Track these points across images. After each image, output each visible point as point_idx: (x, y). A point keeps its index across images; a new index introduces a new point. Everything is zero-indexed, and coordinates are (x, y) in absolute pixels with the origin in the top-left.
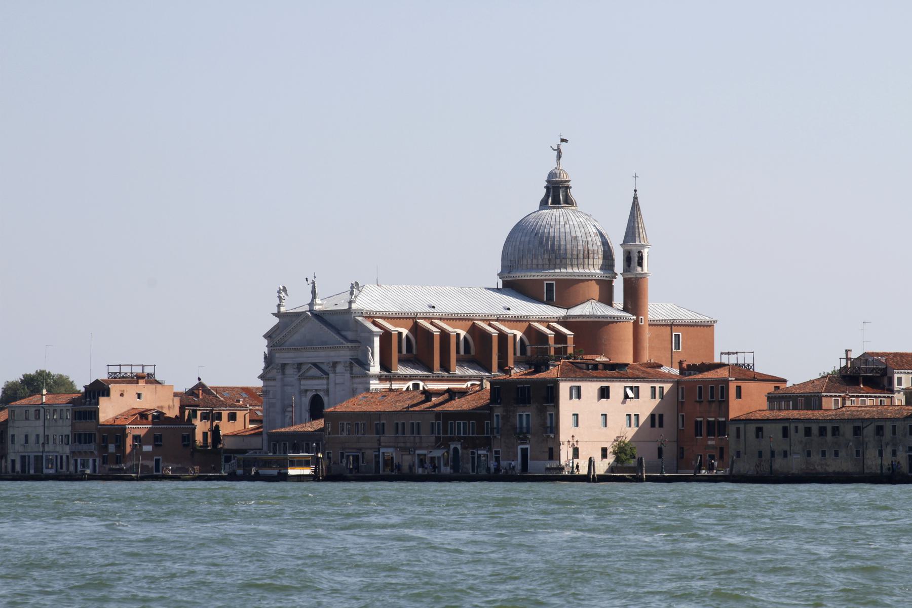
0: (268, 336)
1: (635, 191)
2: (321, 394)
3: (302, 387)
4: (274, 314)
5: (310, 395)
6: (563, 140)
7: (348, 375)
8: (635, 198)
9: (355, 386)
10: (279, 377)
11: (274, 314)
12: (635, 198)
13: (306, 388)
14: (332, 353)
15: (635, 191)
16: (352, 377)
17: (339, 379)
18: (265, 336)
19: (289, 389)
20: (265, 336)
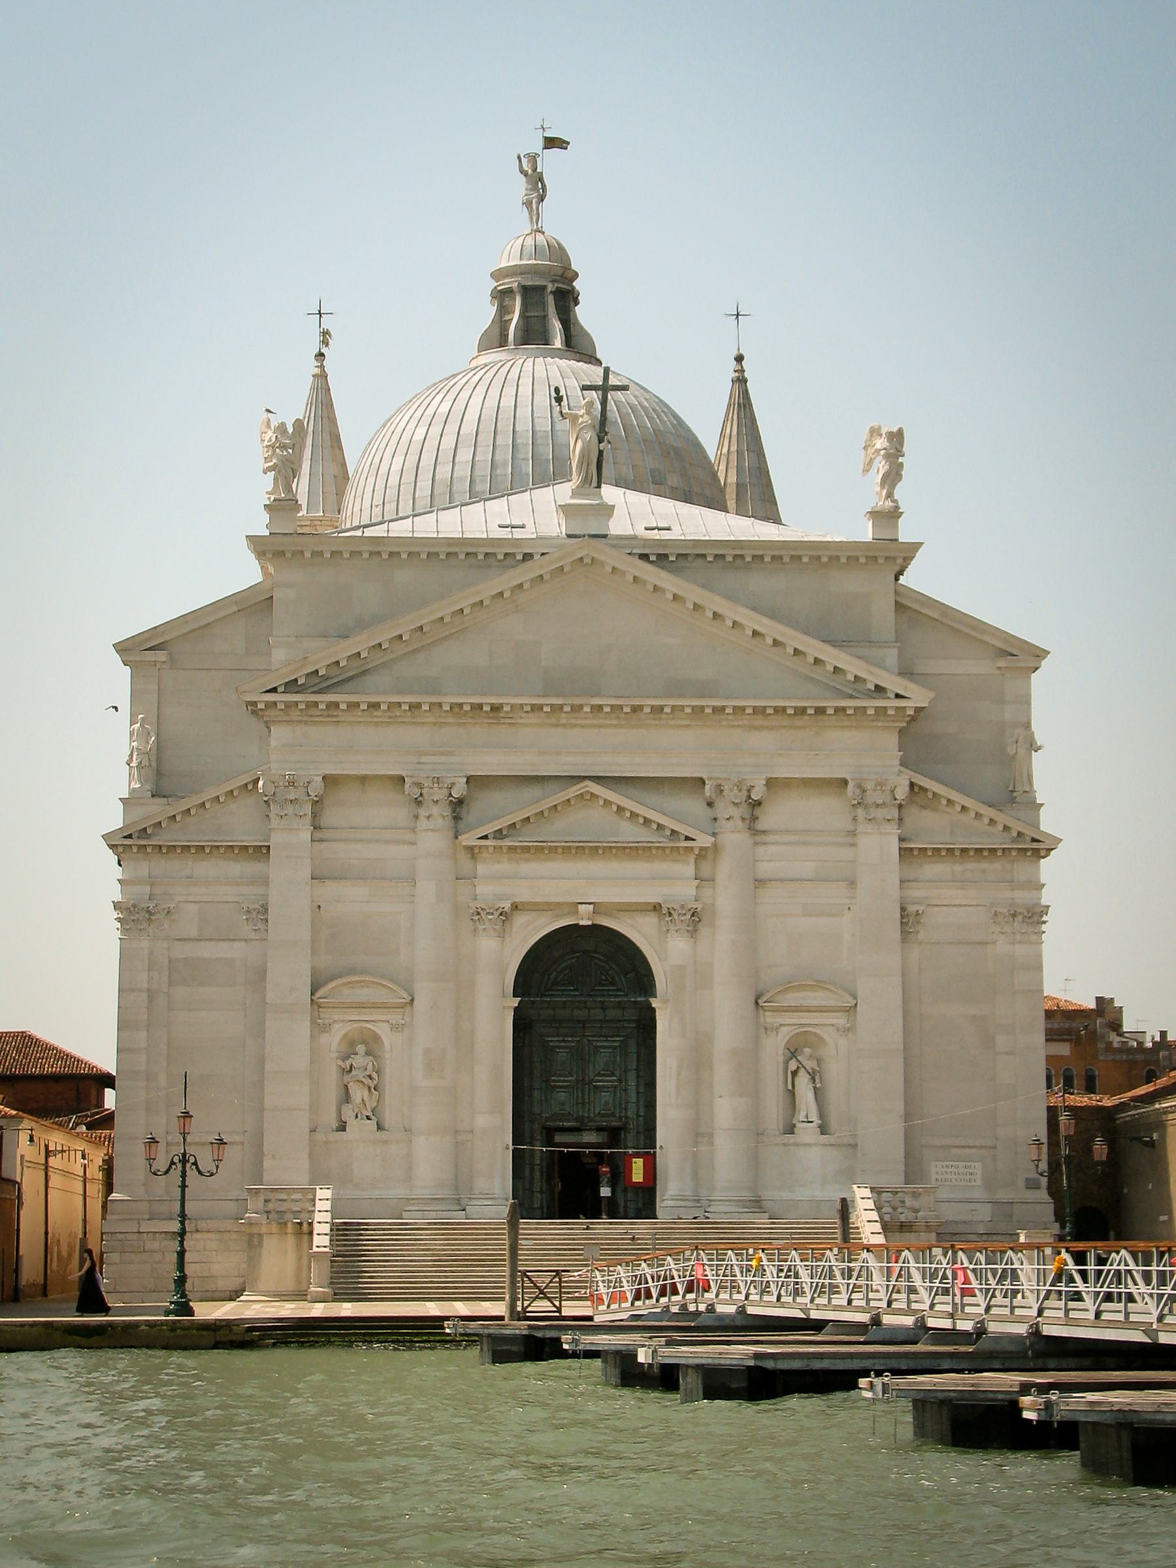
0: (147, 652)
1: (739, 359)
2: (639, 932)
3: (485, 890)
4: (254, 542)
5: (529, 932)
6: (551, 143)
7: (879, 845)
8: (741, 381)
9: (916, 892)
10: (292, 837)
11: (254, 542)
12: (741, 381)
13: (523, 896)
14: (764, 740)
15: (739, 359)
16: (905, 853)
17: (774, 859)
18: (124, 649)
19: (351, 900)
20: (124, 649)
